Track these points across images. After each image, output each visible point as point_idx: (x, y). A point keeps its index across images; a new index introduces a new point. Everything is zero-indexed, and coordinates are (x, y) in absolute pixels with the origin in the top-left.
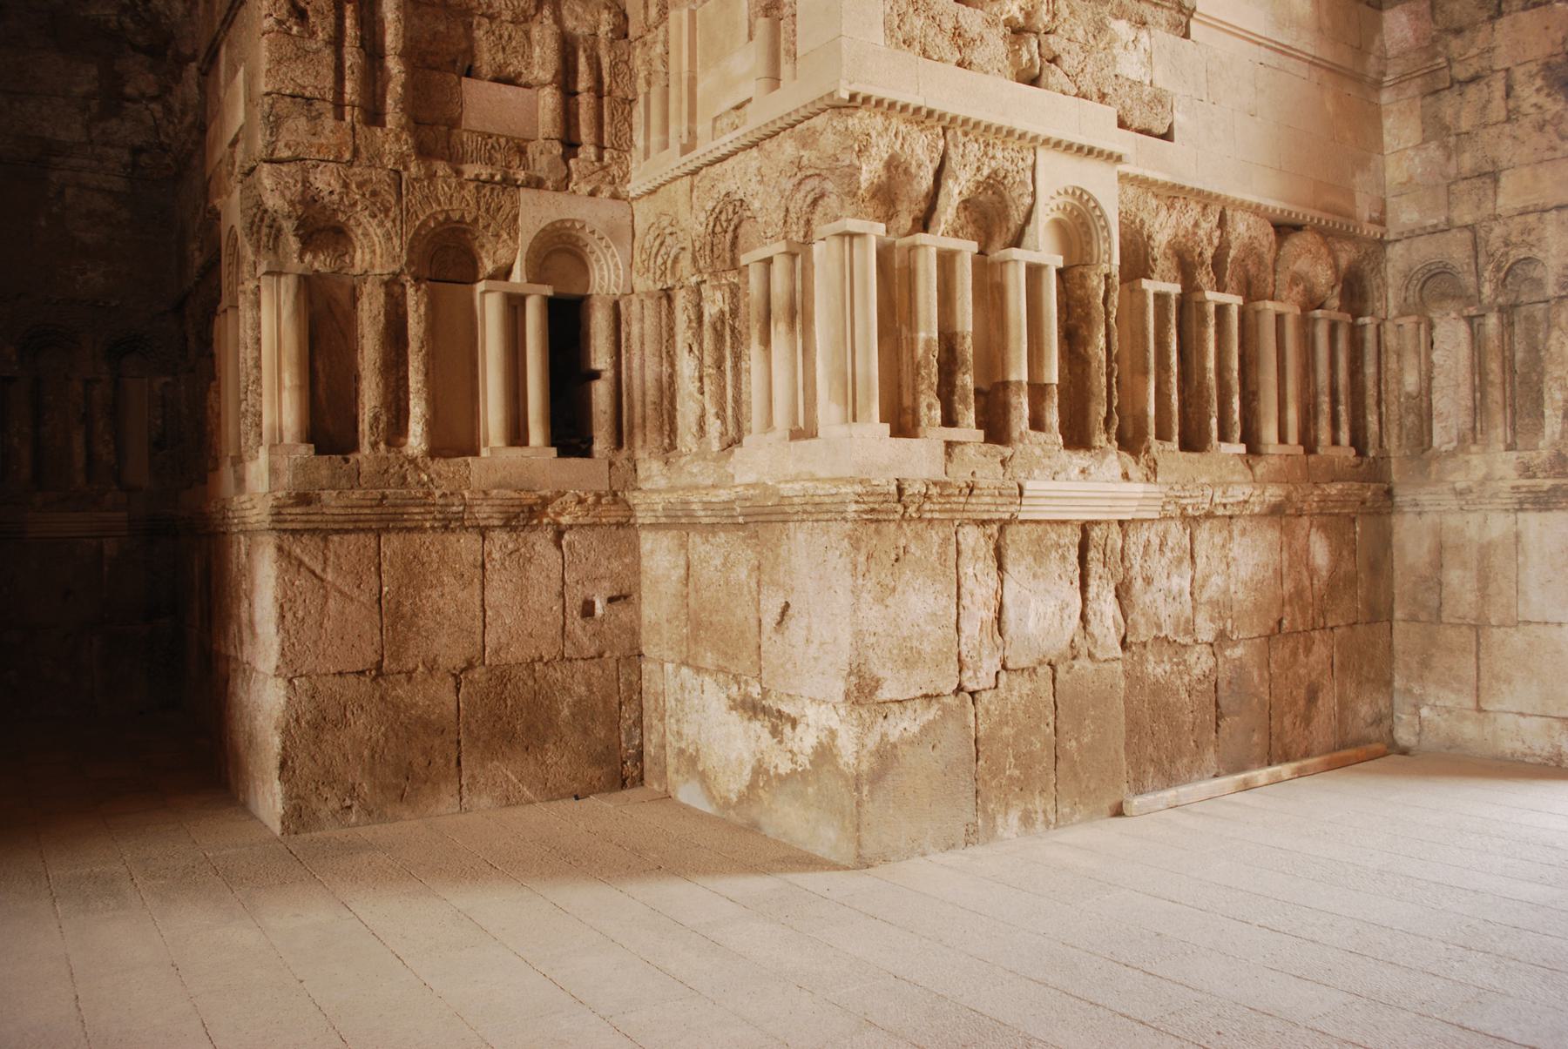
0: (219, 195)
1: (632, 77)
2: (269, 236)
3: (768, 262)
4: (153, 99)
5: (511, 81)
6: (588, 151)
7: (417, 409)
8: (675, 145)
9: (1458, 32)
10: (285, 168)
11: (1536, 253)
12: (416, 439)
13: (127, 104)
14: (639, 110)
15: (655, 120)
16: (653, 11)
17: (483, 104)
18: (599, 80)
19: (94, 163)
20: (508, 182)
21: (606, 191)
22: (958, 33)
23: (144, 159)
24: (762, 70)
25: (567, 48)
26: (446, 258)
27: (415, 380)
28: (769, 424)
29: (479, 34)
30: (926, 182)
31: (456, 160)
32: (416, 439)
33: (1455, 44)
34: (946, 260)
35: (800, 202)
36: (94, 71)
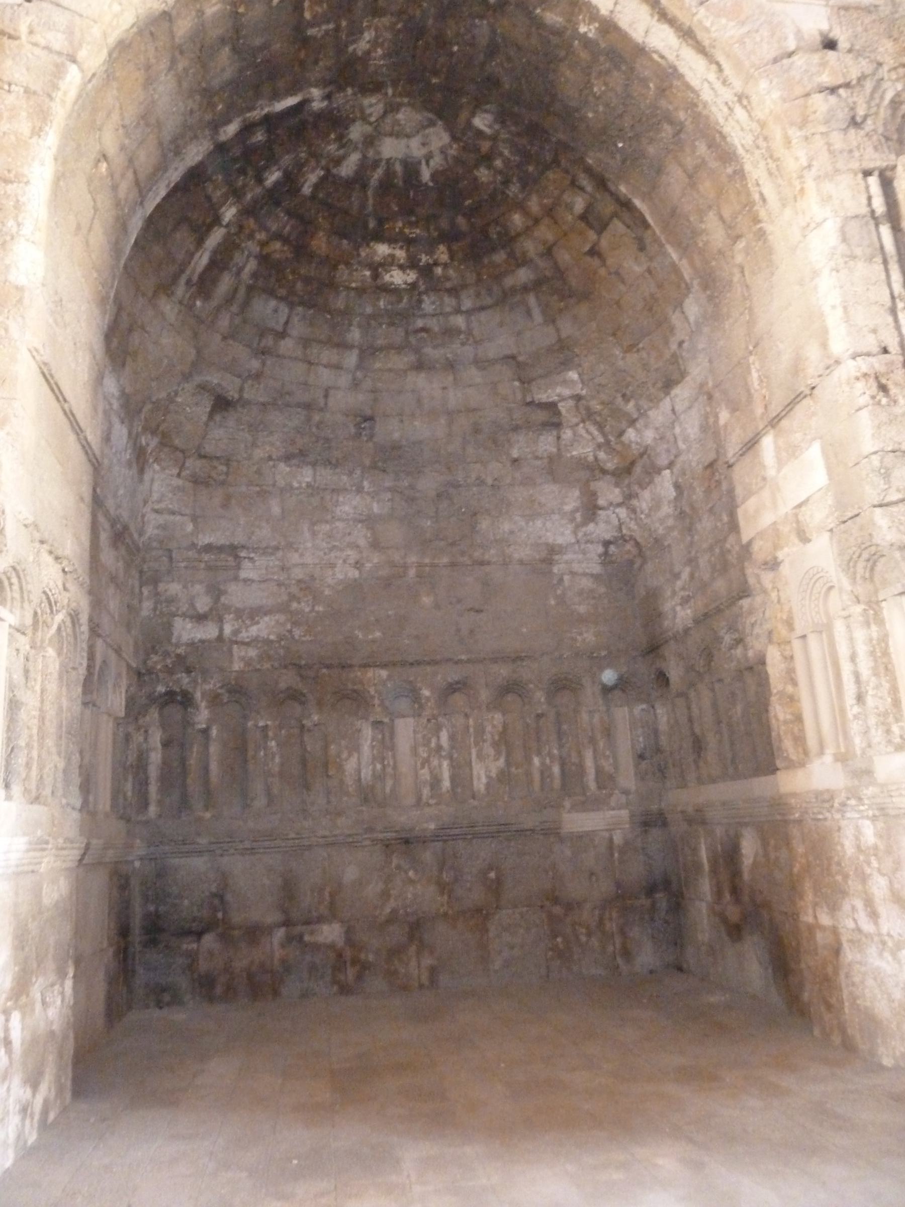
2: (865, 568)
4: (619, 505)
10: (894, 509)
13: (600, 512)
19: (580, 556)
23: (612, 548)
36: (577, 493)
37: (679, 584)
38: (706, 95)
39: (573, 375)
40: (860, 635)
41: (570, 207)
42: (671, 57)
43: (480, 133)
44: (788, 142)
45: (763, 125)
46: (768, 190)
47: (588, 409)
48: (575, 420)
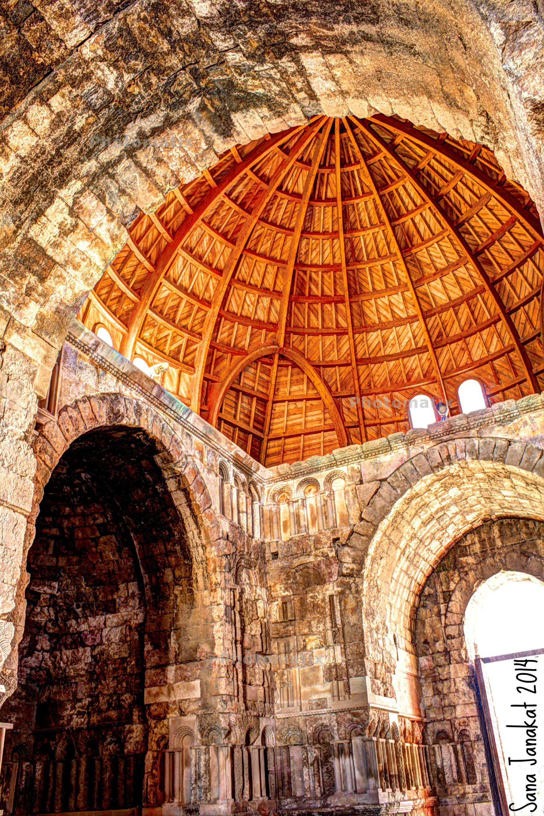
4: (47, 651)
9: (440, 666)
11: (468, 728)
33: (440, 670)
37: (79, 704)
38: (190, 535)
39: (55, 584)
40: (203, 757)
41: (95, 519)
42: (184, 517)
43: (80, 478)
44: (215, 570)
45: (207, 559)
46: (200, 579)
47: (55, 602)
48: (44, 604)
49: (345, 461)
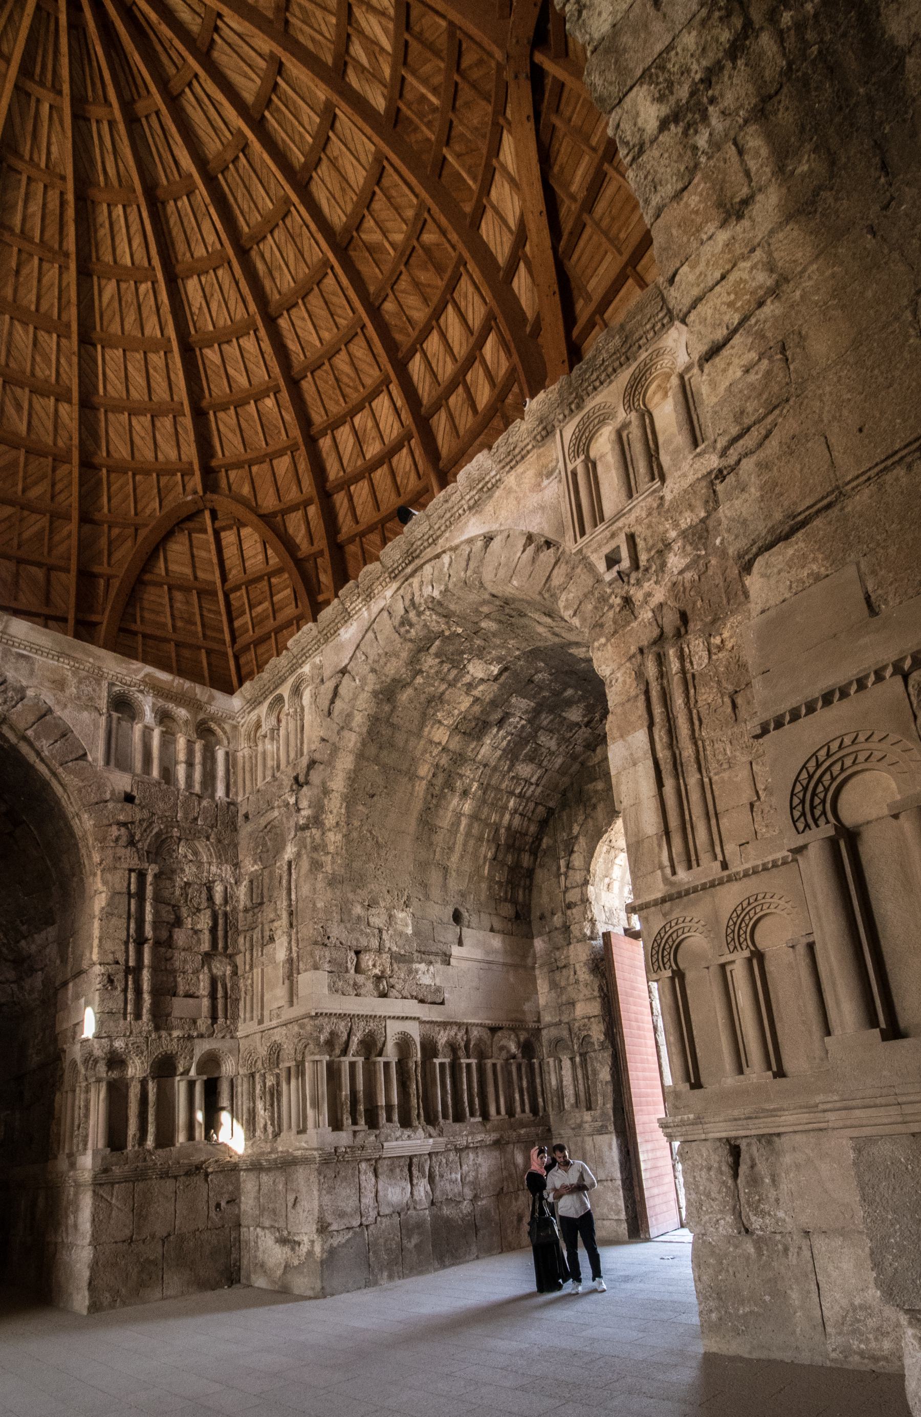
0: (65, 1043)
1: (239, 990)
3: (289, 1068)
5: (191, 996)
6: (221, 1020)
7: (151, 1129)
8: (256, 1020)
12: (150, 1142)
14: (242, 1004)
15: (248, 1008)
16: (247, 967)
17: (179, 1007)
18: (226, 993)
20: (190, 1038)
21: (228, 1036)
22: (355, 984)
24: (286, 998)
25: (213, 981)
26: (164, 1068)
27: (151, 1118)
28: (290, 1127)
29: (179, 979)
30: (344, 1037)
31: (169, 1029)
32: (150, 1142)
34: (353, 1065)
35: (300, 1046)
49: (304, 655)
